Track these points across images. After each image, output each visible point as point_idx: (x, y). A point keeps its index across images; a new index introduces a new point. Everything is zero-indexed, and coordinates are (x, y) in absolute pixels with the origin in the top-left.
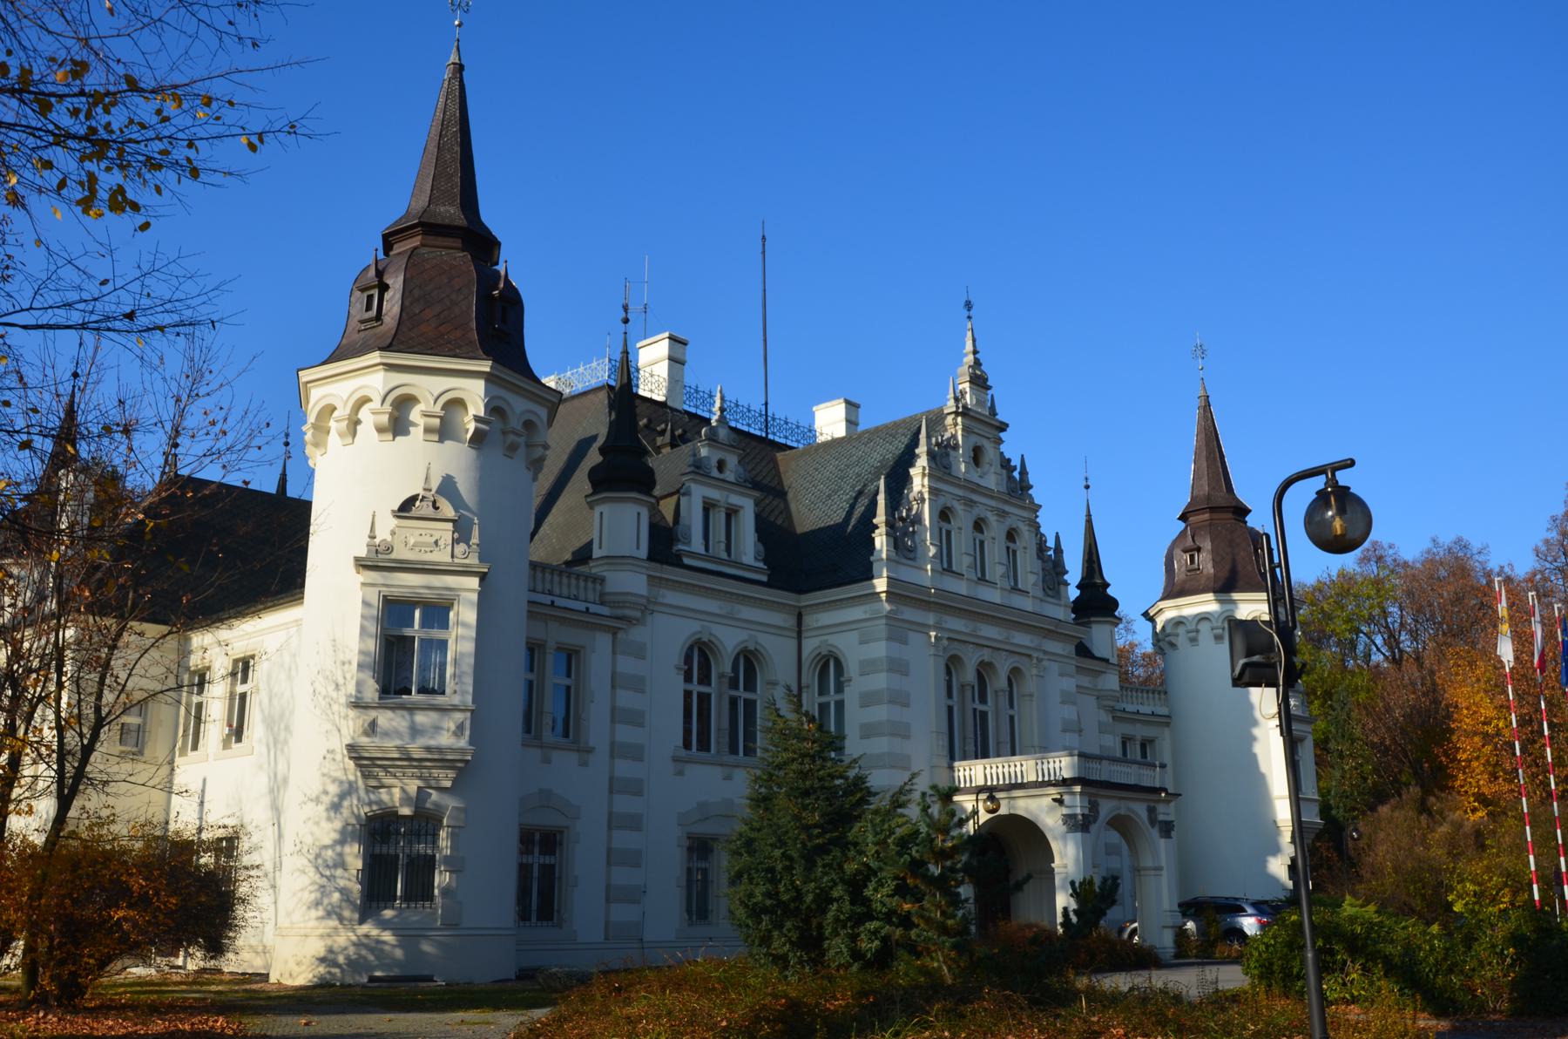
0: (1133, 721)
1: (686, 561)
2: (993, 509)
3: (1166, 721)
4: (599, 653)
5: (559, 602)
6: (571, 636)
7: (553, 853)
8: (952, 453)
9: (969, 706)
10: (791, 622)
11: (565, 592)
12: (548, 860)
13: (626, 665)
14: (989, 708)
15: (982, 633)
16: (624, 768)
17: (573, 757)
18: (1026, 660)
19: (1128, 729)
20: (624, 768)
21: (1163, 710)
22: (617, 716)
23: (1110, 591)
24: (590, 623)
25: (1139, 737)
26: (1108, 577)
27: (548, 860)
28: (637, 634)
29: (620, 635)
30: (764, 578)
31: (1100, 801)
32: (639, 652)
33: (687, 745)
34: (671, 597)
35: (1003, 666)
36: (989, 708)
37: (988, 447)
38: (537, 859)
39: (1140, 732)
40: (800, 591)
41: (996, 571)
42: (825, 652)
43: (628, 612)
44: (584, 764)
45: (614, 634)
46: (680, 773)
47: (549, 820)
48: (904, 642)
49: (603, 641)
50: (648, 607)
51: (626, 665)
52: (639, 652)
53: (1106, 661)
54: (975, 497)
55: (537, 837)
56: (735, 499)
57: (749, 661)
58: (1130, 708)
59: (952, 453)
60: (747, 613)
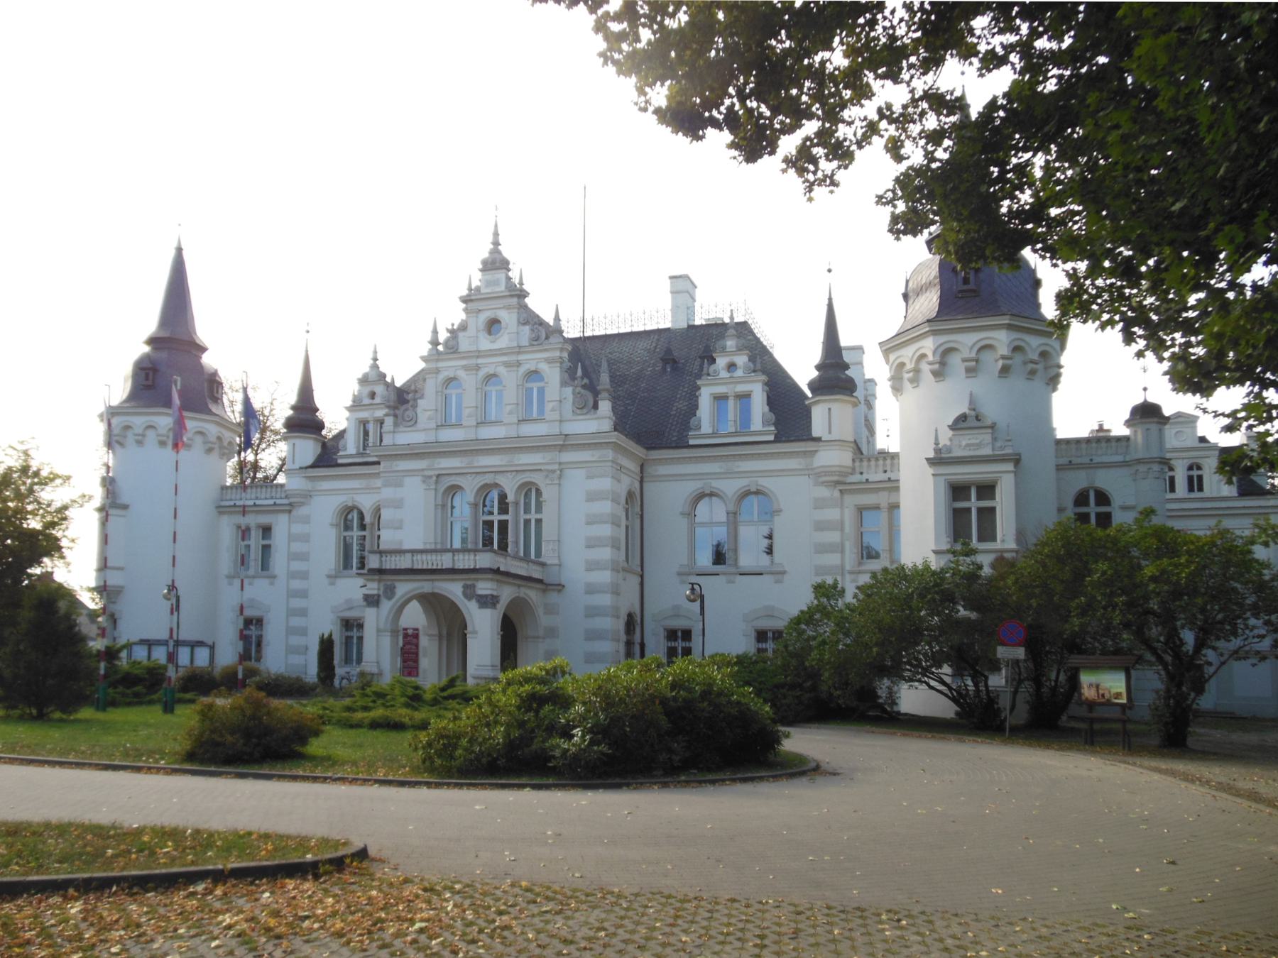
4: (281, 525)
6: (264, 519)
8: (461, 334)
9: (523, 517)
13: (297, 528)
17: (267, 581)
24: (275, 509)
31: (397, 584)
34: (326, 485)
42: (350, 504)
43: (292, 500)
50: (307, 496)
51: (297, 528)
53: (818, 440)
54: (480, 361)
58: (874, 477)
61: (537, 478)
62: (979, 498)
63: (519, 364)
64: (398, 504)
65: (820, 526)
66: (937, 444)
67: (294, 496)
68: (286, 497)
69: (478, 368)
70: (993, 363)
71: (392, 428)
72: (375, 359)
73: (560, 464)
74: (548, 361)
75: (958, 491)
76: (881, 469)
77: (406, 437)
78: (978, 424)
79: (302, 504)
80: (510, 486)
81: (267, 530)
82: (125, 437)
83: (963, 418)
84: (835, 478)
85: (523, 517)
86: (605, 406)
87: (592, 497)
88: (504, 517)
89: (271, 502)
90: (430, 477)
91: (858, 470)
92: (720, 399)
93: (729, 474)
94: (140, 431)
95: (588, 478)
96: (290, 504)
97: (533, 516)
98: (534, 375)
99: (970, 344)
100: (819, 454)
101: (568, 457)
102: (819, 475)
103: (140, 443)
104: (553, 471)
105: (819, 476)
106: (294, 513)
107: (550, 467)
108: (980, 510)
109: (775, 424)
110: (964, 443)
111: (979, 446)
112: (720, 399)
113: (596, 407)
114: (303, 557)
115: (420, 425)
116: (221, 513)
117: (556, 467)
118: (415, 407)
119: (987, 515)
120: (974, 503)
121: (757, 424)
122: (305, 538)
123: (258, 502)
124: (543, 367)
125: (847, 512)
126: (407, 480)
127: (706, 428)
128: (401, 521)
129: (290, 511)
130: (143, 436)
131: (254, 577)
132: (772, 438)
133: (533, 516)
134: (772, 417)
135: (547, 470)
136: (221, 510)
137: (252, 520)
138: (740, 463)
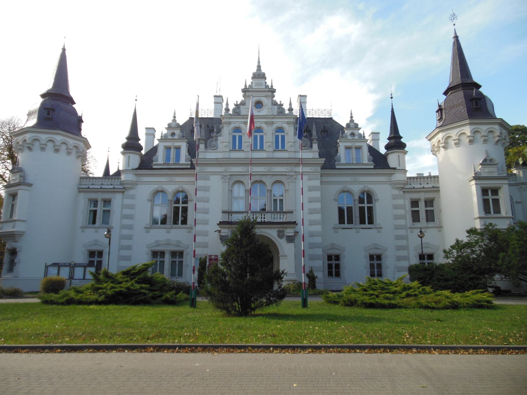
0: (419, 192)
1: (154, 167)
2: (266, 123)
4: (117, 200)
5: (116, 187)
6: (106, 196)
11: (109, 183)
13: (127, 201)
15: (275, 170)
18: (285, 177)
23: (402, 140)
24: (114, 191)
26: (401, 134)
27: (378, 262)
28: (132, 192)
29: (125, 193)
30: (189, 167)
32: (133, 197)
34: (146, 179)
37: (264, 100)
38: (375, 262)
43: (125, 186)
46: (147, 232)
47: (378, 252)
48: (208, 180)
50: (134, 184)
51: (127, 201)
52: (133, 197)
53: (395, 169)
55: (375, 257)
56: (177, 144)
59: (242, 107)
60: (178, 179)
62: (492, 195)
63: (273, 123)
64: (206, 189)
65: (396, 207)
66: (475, 171)
68: (121, 185)
70: (465, 140)
71: (204, 150)
72: (175, 117)
73: (295, 172)
74: (288, 123)
75: (484, 191)
76: (426, 183)
77: (211, 155)
78: (491, 163)
79: (131, 188)
81: (107, 202)
82: (33, 145)
83: (485, 160)
84: (402, 186)
86: (315, 146)
89: (112, 187)
91: (409, 183)
92: (348, 148)
93: (355, 182)
94: (44, 143)
95: (309, 180)
96: (124, 188)
98: (280, 130)
99: (485, 130)
100: (394, 175)
101: (300, 169)
102: (395, 184)
103: (43, 149)
104: (292, 176)
106: (126, 193)
107: (291, 174)
108: (368, 207)
109: (373, 161)
110: (486, 171)
111: (492, 172)
112: (348, 148)
113: (311, 147)
114: (130, 217)
115: (218, 150)
116: (79, 192)
117: (294, 174)
118: (216, 140)
119: (496, 202)
120: (490, 197)
121: (366, 161)
122: (132, 207)
123: (103, 187)
124: (285, 126)
125: (407, 200)
126: (212, 177)
127: (343, 161)
128: (208, 198)
129: (123, 192)
130: (46, 145)
131: (99, 228)
132: (372, 167)
134: (371, 158)
135: (289, 175)
136: (80, 190)
137: (100, 197)
138: (360, 178)
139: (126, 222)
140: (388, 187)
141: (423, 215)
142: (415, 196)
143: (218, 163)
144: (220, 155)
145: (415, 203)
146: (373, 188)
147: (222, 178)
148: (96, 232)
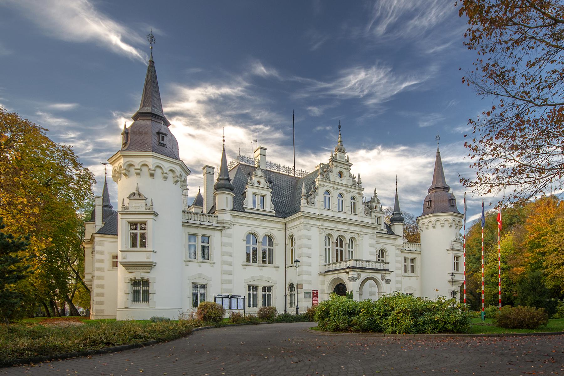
3: (419, 252)
7: (256, 291)
10: (283, 226)
12: (254, 293)
13: (226, 240)
14: (331, 247)
16: (226, 268)
19: (406, 255)
20: (226, 268)
21: (418, 250)
22: (223, 254)
25: (410, 258)
32: (230, 236)
33: (248, 260)
35: (348, 237)
36: (331, 247)
39: (410, 256)
40: (285, 218)
41: (347, 209)
44: (212, 267)
45: (222, 231)
49: (218, 234)
51: (226, 240)
52: (230, 236)
57: (270, 239)
58: (407, 249)
61: (355, 236)
67: (226, 223)
69: (350, 192)
71: (306, 205)
80: (348, 237)
81: (206, 238)
85: (348, 249)
87: (371, 246)
88: (341, 249)
90: (322, 229)
97: (351, 250)
105: (396, 246)
115: (316, 207)
117: (362, 233)
122: (230, 245)
133: (339, 248)
139: (226, 258)
140: (393, 248)
141: (409, 268)
142: (406, 255)
143: (318, 218)
144: (316, 211)
145: (405, 259)
146: (387, 247)
147: (320, 231)
148: (200, 266)
